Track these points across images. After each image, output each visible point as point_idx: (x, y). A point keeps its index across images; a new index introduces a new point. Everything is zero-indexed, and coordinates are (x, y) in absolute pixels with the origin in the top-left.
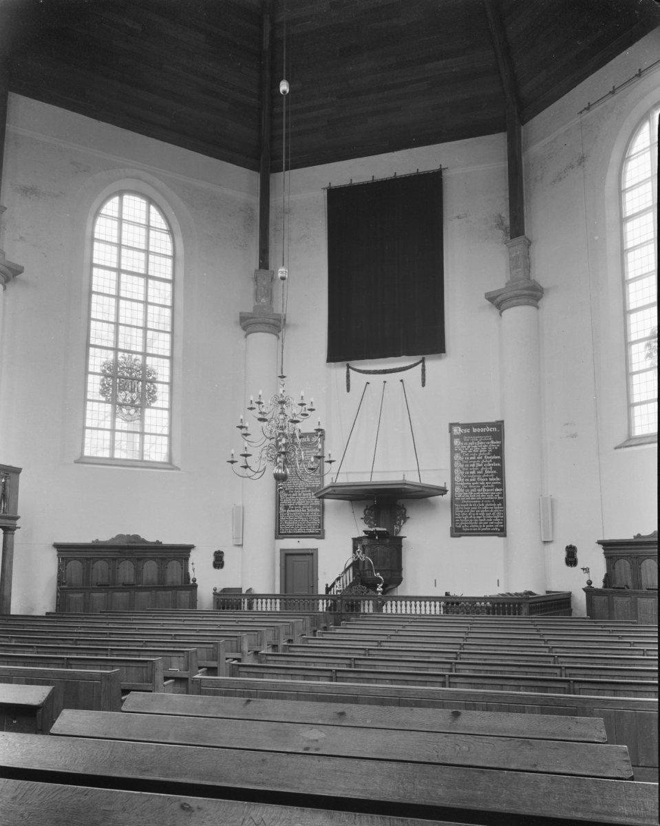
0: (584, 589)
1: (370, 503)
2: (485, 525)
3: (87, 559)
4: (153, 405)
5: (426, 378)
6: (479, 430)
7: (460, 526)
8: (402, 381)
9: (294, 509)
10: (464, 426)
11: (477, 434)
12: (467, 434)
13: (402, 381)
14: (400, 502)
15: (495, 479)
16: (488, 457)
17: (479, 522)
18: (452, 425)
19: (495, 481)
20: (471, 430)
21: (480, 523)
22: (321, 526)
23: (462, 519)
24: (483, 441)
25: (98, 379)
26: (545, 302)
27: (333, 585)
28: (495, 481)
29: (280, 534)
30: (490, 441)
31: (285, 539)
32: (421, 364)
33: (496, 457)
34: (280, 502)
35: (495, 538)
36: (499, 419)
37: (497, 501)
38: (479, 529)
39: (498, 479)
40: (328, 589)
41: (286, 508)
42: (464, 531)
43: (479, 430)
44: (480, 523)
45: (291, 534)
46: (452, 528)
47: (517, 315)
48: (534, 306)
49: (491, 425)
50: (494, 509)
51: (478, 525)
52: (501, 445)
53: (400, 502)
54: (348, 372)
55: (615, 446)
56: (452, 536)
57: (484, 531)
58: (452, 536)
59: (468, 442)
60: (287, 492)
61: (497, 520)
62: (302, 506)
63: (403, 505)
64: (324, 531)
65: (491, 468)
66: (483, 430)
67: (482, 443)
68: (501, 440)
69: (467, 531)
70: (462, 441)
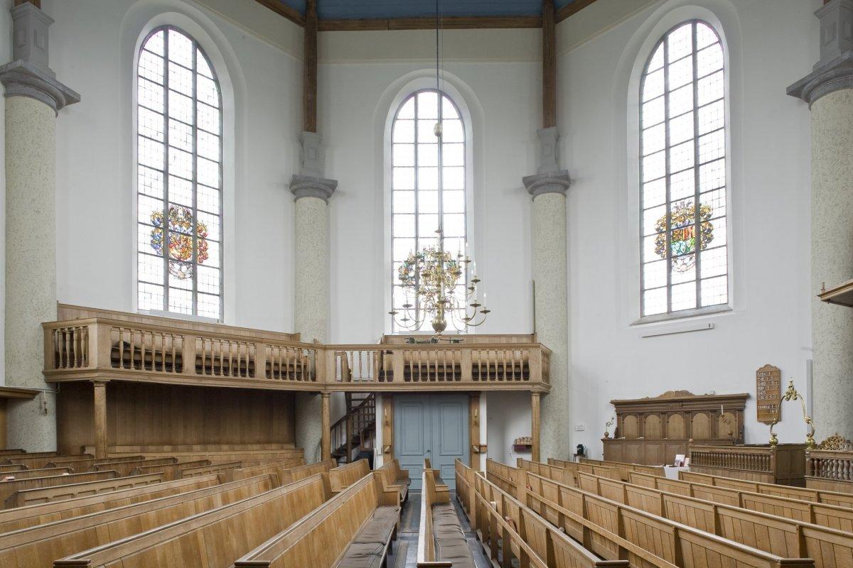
0: (602, 440)
3: (663, 413)
4: (205, 262)
25: (149, 230)
26: (572, 192)
47: (549, 200)
48: (561, 193)
55: (631, 322)
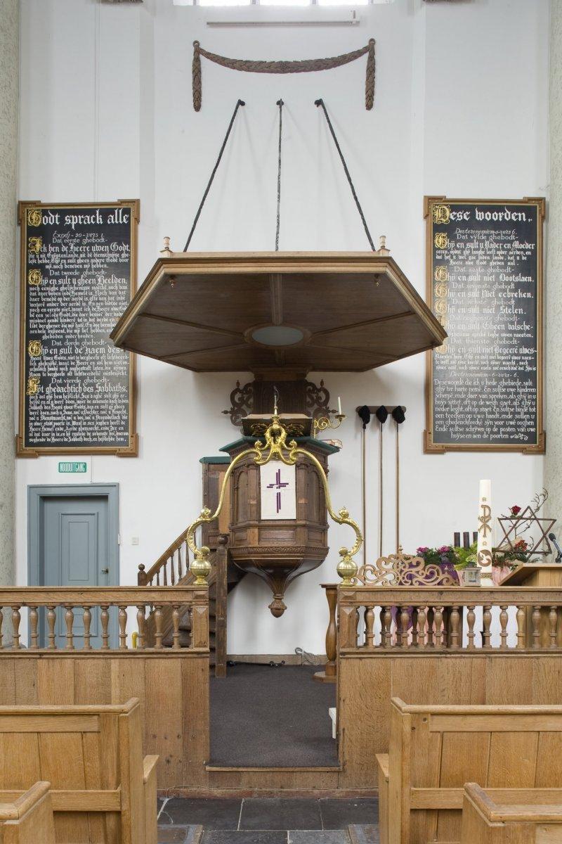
1: (246, 377)
2: (498, 427)
5: (377, 89)
6: (488, 216)
7: (444, 429)
8: (319, 103)
9: (64, 385)
10: (456, 206)
11: (484, 225)
12: (464, 224)
13: (319, 103)
14: (313, 377)
15: (519, 328)
16: (507, 279)
17: (484, 420)
18: (431, 202)
19: (521, 332)
20: (472, 215)
21: (487, 423)
22: (130, 425)
23: (450, 413)
24: (497, 241)
27: (156, 569)
28: (521, 332)
29: (28, 444)
30: (511, 242)
31: (43, 459)
32: (365, 57)
33: (524, 279)
34: (28, 367)
35: (518, 456)
36: (532, 193)
37: (524, 376)
38: (485, 436)
39: (527, 327)
40: (144, 577)
41: (45, 381)
42: (453, 441)
43: (488, 216)
44: (487, 423)
45: (57, 444)
46: (426, 433)
49: (515, 206)
50: (516, 393)
51: (483, 426)
52: (534, 252)
53: (313, 377)
54: (197, 61)
56: (428, 450)
57: (496, 441)
58: (428, 450)
59: (465, 242)
60: (46, 344)
61: (523, 416)
62: (82, 378)
63: (322, 383)
64: (136, 436)
65: (513, 302)
66: (497, 216)
67: (495, 246)
68: (532, 239)
69: (461, 441)
70: (452, 237)
